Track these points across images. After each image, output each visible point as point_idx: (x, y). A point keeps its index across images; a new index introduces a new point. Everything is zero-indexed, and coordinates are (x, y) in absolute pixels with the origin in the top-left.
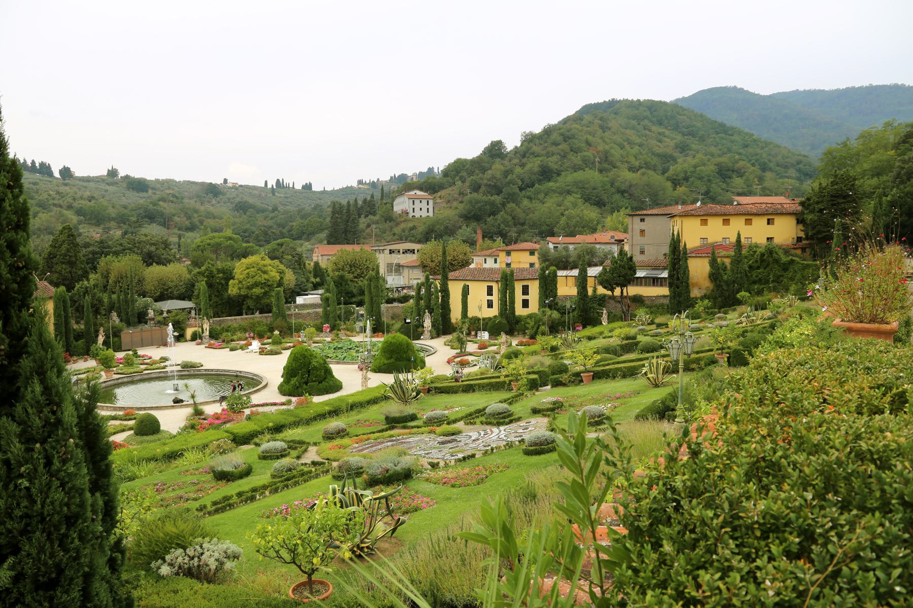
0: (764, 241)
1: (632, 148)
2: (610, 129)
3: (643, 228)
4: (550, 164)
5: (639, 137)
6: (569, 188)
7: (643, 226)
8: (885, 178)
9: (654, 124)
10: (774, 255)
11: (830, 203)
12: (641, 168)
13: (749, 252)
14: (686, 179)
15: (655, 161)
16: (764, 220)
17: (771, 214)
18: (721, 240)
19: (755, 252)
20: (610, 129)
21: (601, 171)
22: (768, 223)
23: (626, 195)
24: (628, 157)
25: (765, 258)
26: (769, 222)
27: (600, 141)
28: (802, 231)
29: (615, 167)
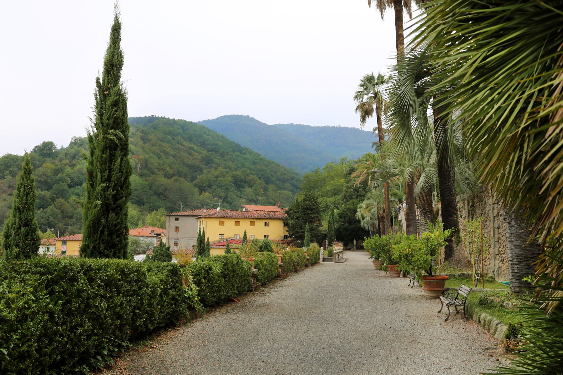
0: (263, 238)
1: (167, 158)
2: (149, 141)
3: (177, 225)
5: (174, 149)
7: (177, 224)
8: (338, 197)
9: (185, 140)
12: (174, 175)
15: (186, 170)
18: (233, 236)
20: (149, 141)
22: (265, 225)
23: (162, 196)
28: (287, 231)
29: (153, 173)
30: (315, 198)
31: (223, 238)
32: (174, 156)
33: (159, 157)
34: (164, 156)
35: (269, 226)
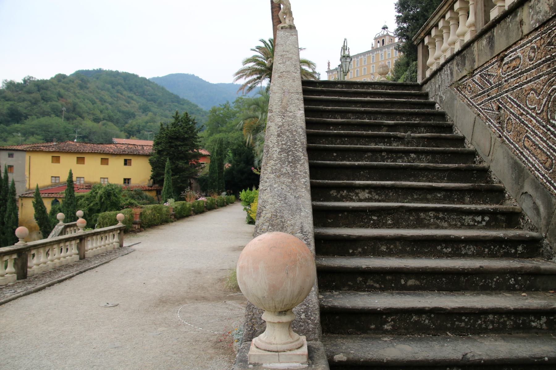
0: (122, 182)
1: (102, 105)
2: (88, 88)
3: (11, 164)
4: (20, 108)
5: (111, 97)
6: (32, 130)
9: (125, 90)
10: (113, 198)
11: (168, 145)
12: (104, 119)
13: (91, 193)
14: (139, 131)
16: (121, 161)
17: (127, 155)
19: (97, 193)
20: (88, 88)
21: (68, 119)
22: (125, 164)
23: (86, 140)
24: (94, 110)
25: (103, 200)
26: (126, 163)
27: (71, 94)
29: (81, 117)
30: (191, 123)
31: (57, 181)
32: (111, 104)
33: (94, 103)
34: (99, 102)
35: (130, 165)
